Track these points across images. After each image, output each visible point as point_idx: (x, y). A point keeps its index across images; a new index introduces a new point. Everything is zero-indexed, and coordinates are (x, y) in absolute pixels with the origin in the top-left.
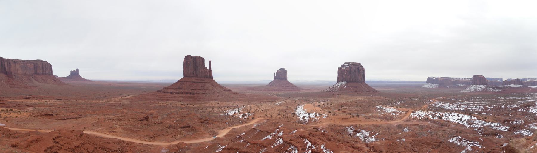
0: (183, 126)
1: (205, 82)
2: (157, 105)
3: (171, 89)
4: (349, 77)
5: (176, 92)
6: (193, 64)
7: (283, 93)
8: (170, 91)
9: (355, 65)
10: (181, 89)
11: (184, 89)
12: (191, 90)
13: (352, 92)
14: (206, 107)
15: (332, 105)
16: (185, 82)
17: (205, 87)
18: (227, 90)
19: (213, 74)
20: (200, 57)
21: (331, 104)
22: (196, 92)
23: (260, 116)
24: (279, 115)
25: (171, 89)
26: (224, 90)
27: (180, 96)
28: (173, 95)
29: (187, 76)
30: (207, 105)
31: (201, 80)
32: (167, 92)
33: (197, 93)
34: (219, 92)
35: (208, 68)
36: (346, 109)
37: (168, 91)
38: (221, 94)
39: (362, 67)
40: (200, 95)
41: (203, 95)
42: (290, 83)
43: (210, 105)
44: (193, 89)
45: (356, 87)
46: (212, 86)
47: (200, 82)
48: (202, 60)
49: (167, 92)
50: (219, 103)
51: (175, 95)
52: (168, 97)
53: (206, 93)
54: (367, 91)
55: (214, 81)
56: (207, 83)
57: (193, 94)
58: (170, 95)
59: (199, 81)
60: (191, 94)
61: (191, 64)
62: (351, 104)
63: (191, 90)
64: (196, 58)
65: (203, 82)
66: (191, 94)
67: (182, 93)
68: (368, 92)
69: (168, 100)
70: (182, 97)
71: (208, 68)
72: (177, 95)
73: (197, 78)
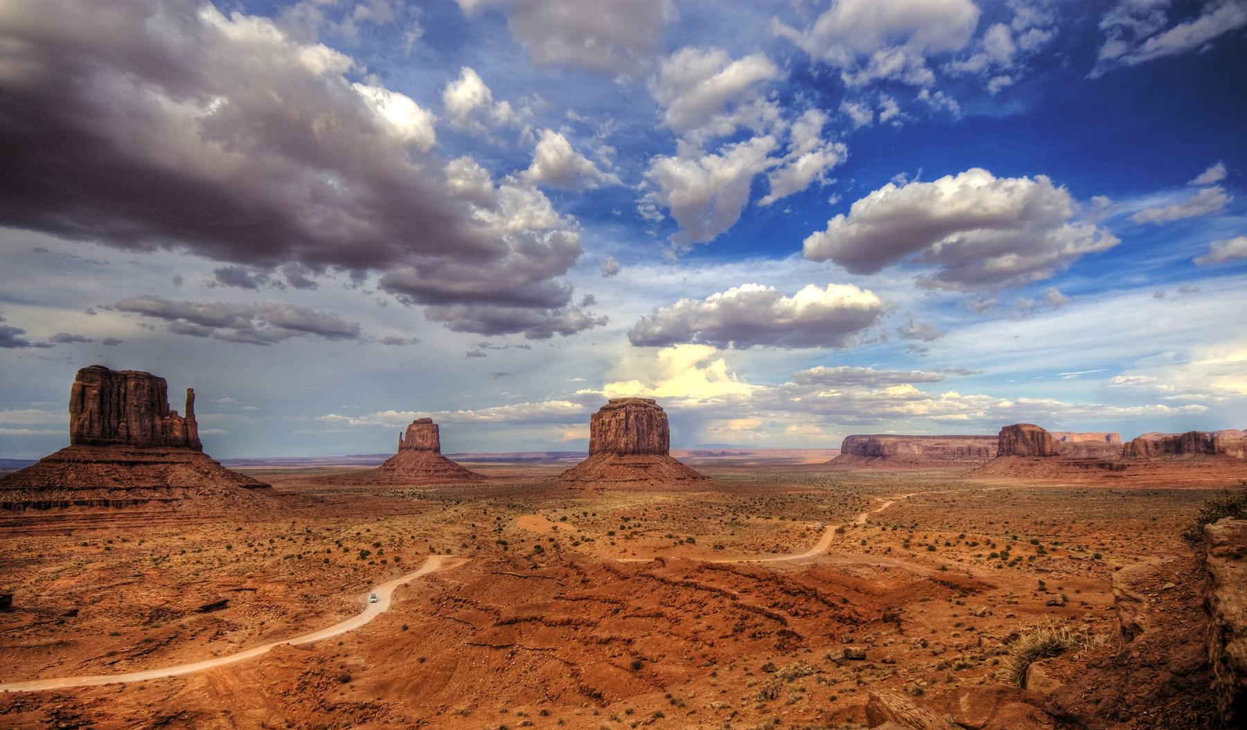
1: (173, 463)
4: (624, 440)
7: (432, 490)
9: (641, 406)
10: (61, 488)
12: (111, 490)
31: (158, 455)
39: (662, 410)
44: (116, 489)
45: (646, 467)
53: (177, 500)
54: (678, 479)
55: (208, 457)
56: (177, 466)
63: (111, 490)
65: (164, 463)
67: (65, 505)
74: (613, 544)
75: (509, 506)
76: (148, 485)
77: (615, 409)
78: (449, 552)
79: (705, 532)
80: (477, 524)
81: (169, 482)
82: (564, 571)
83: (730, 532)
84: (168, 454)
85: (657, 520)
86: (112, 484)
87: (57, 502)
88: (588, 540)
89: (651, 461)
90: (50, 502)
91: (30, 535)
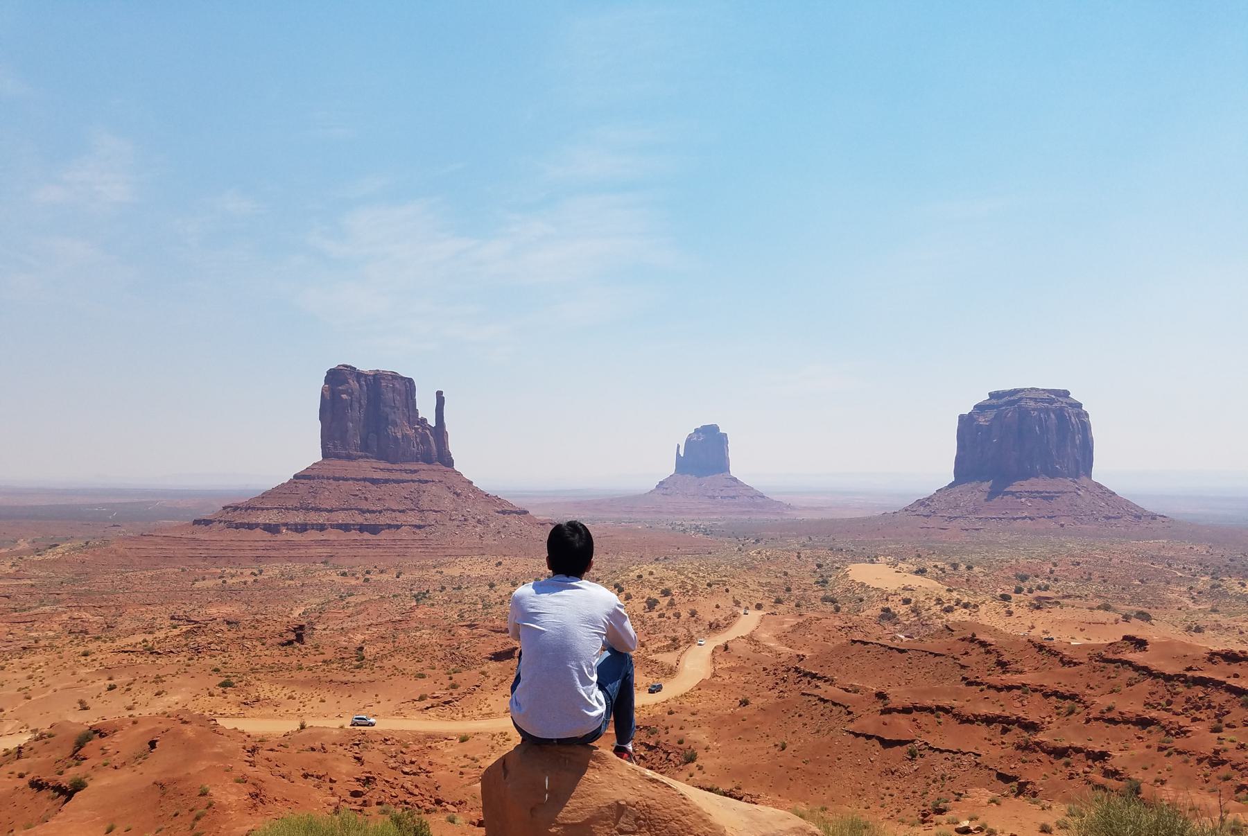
0: (491, 650)
1: (420, 481)
2: (230, 581)
3: (267, 509)
5: (291, 521)
6: (364, 402)
8: (262, 518)
11: (331, 511)
12: (363, 512)
13: (1030, 518)
14: (453, 578)
15: (976, 569)
16: (331, 481)
17: (425, 502)
18: (512, 512)
19: (455, 447)
20: (395, 377)
21: (969, 568)
22: (382, 520)
23: (718, 607)
24: (779, 601)
25: (267, 509)
26: (504, 512)
27: (316, 541)
28: (279, 537)
29: (338, 457)
30: (455, 572)
31: (405, 471)
32: (251, 527)
33: (389, 526)
34: (482, 518)
35: (432, 422)
36: (1047, 588)
37: (253, 520)
38: (491, 525)
40: (403, 533)
41: (418, 531)
42: (742, 485)
43: (467, 573)
44: (369, 511)
46: (451, 495)
47: (397, 482)
48: (409, 385)
49: (251, 527)
50: (500, 563)
51: (286, 535)
52: (256, 544)
54: (1108, 518)
55: (459, 474)
57: (374, 529)
58: (267, 535)
59: (393, 477)
60: (362, 528)
61: (356, 405)
62: (1053, 568)
63: (363, 512)
64: (377, 377)
65: (413, 481)
66: (362, 528)
67: (322, 528)
68: (1112, 521)
69: (258, 559)
70: (324, 543)
71: (432, 422)
72: (296, 537)
73: (383, 465)
74: (1010, 613)
75: (832, 549)
76: (401, 508)
77: (999, 406)
78: (759, 607)
79: (1163, 604)
80: (790, 572)
81: (420, 503)
82: (961, 647)
83: (1208, 606)
84: (416, 471)
85: (1076, 581)
86: (364, 505)
87: (313, 524)
88: (966, 606)
89: (1060, 488)
90: (306, 525)
91: (291, 561)
